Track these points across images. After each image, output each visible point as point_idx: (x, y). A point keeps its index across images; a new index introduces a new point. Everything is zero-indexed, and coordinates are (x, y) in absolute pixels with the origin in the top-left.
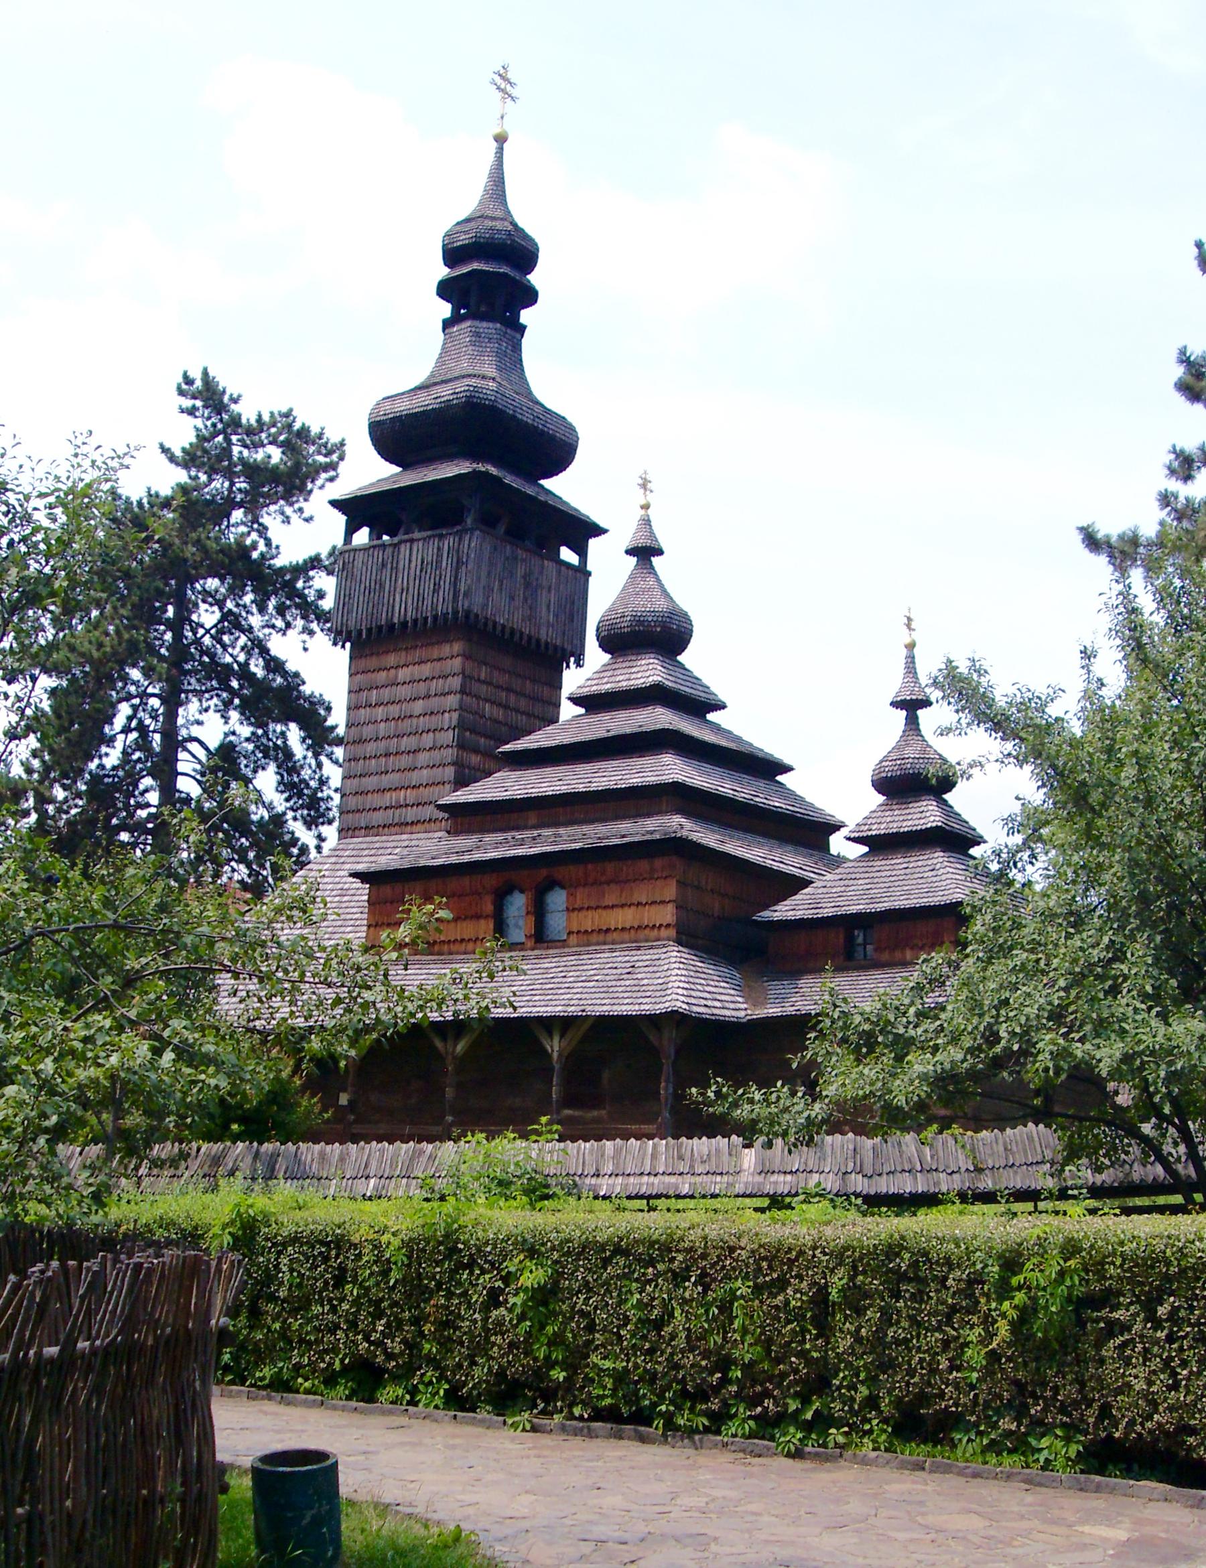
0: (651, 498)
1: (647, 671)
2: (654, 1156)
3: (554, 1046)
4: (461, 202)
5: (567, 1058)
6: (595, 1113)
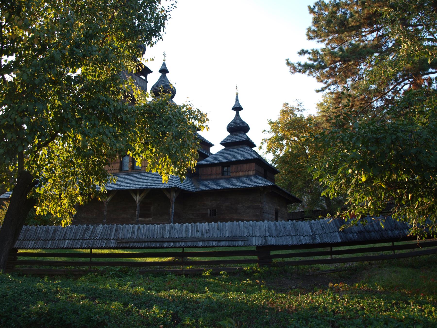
0: (166, 58)
5: (141, 202)
6: (148, 219)
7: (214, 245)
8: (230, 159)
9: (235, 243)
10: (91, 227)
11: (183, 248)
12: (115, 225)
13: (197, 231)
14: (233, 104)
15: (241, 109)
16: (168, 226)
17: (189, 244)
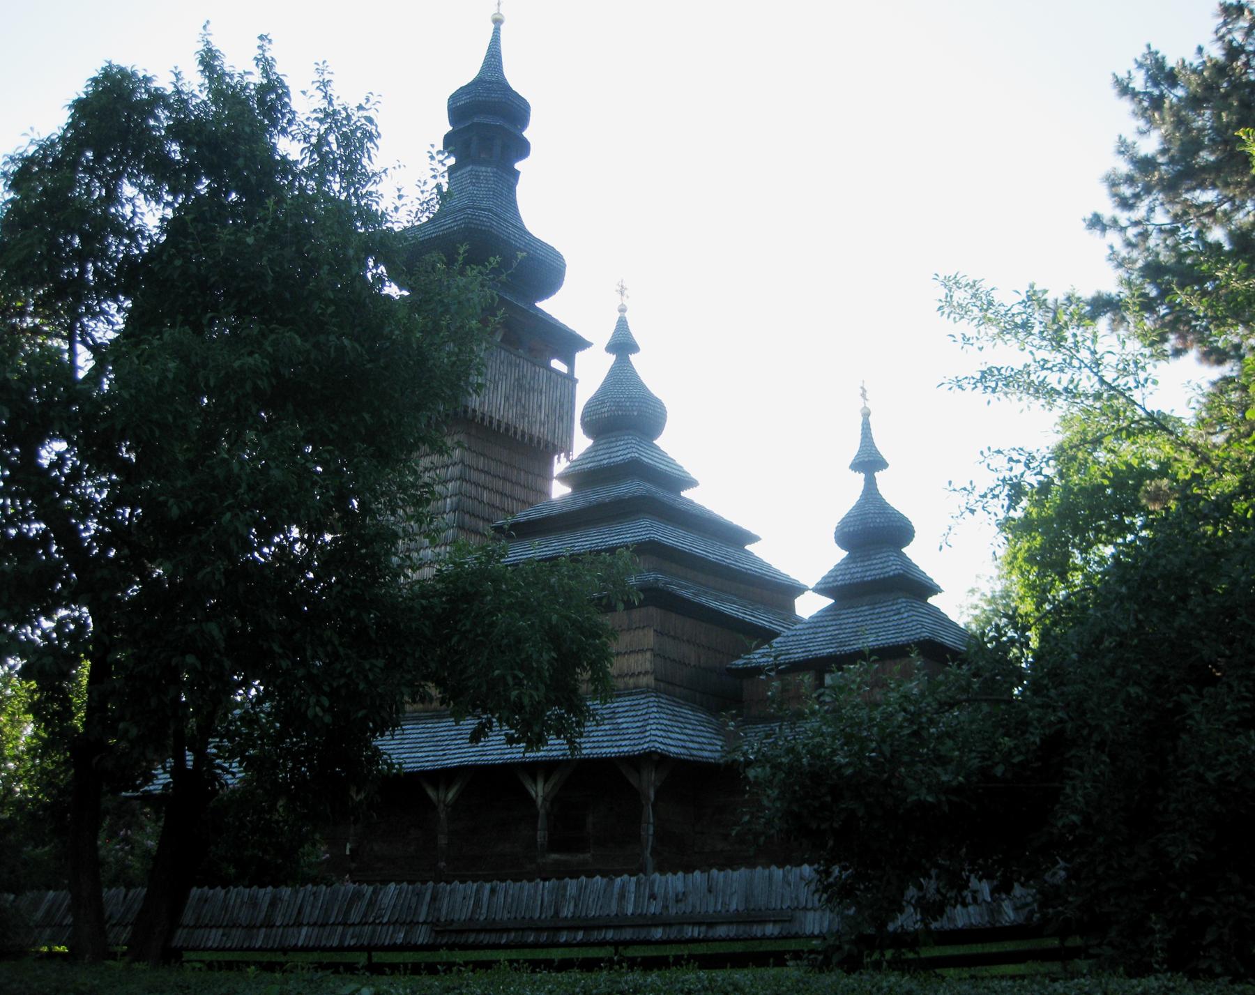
2: (622, 897)
3: (539, 791)
6: (581, 856)
7: (696, 934)
8: (842, 644)
9: (757, 930)
10: (368, 890)
11: (616, 944)
12: (431, 884)
13: (653, 896)
14: (853, 448)
15: (882, 464)
16: (572, 885)
17: (627, 934)
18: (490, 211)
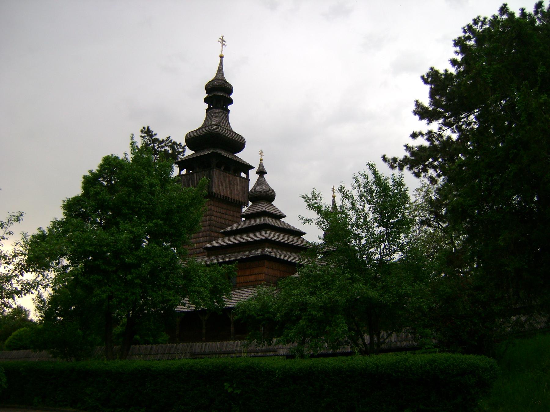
0: (263, 158)
1: (262, 207)
4: (211, 75)
10: (175, 345)
18: (219, 126)
